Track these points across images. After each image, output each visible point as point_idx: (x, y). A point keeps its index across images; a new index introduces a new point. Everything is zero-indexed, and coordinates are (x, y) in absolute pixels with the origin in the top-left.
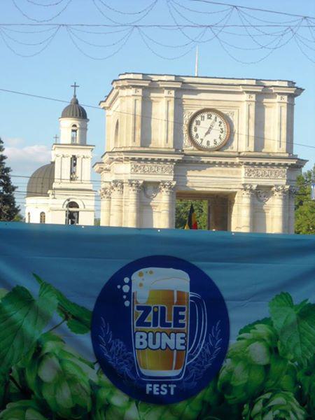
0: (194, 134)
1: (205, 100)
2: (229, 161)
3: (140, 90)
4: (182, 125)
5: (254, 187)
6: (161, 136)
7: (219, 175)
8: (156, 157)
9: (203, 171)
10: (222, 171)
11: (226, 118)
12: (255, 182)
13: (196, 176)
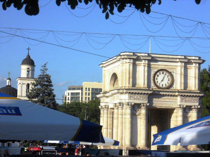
0: (156, 81)
1: (161, 65)
2: (173, 94)
3: (132, 60)
4: (151, 77)
5: (185, 106)
6: (141, 82)
7: (168, 100)
8: (140, 92)
9: (160, 99)
10: (169, 99)
11: (170, 73)
12: (185, 104)
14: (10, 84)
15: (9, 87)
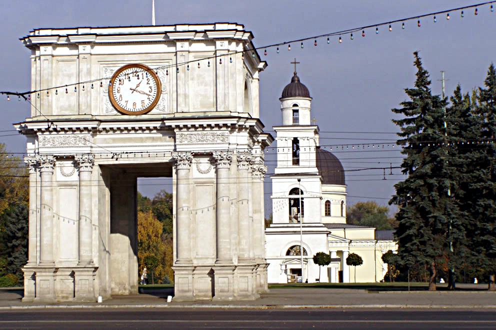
13: (156, 146)
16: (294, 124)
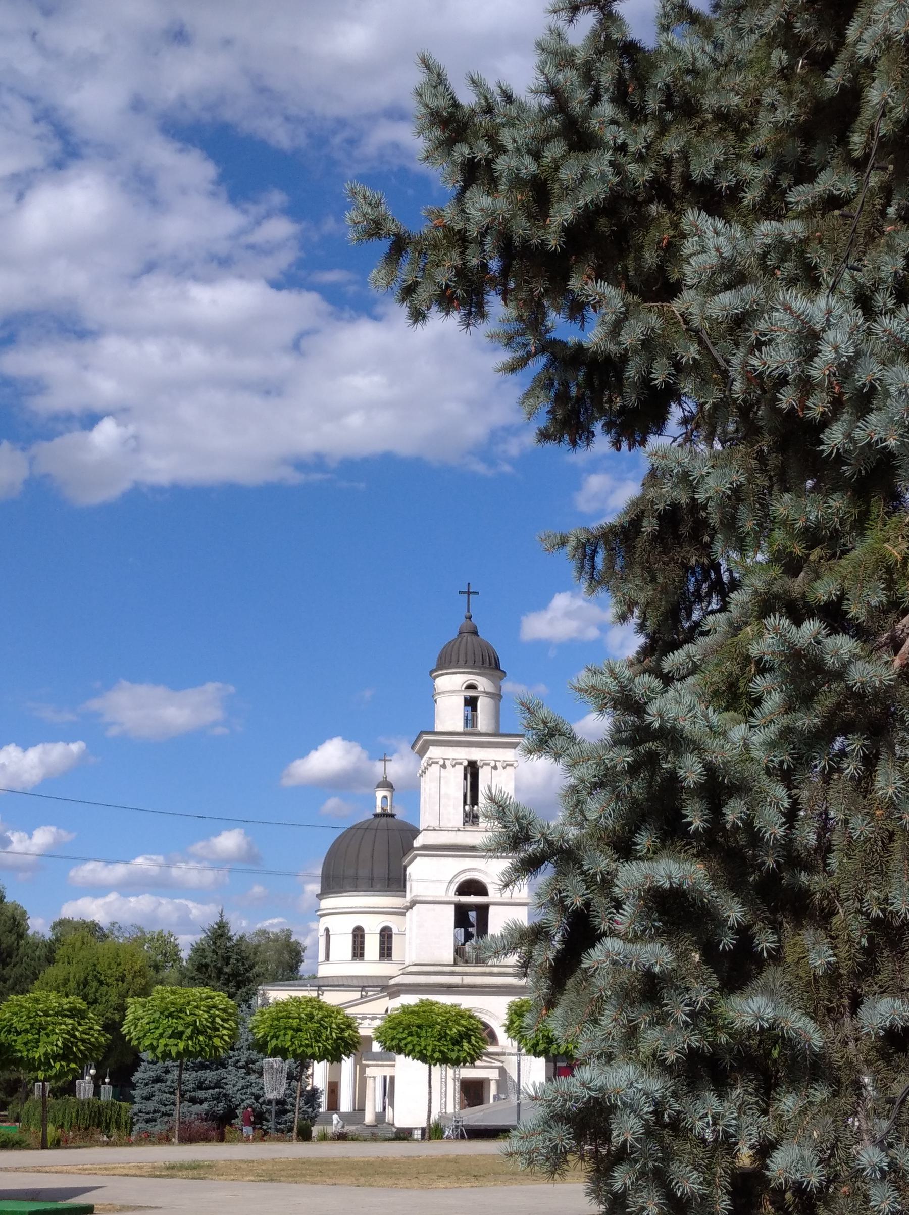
14: (391, 806)
15: (384, 819)
16: (469, 729)
